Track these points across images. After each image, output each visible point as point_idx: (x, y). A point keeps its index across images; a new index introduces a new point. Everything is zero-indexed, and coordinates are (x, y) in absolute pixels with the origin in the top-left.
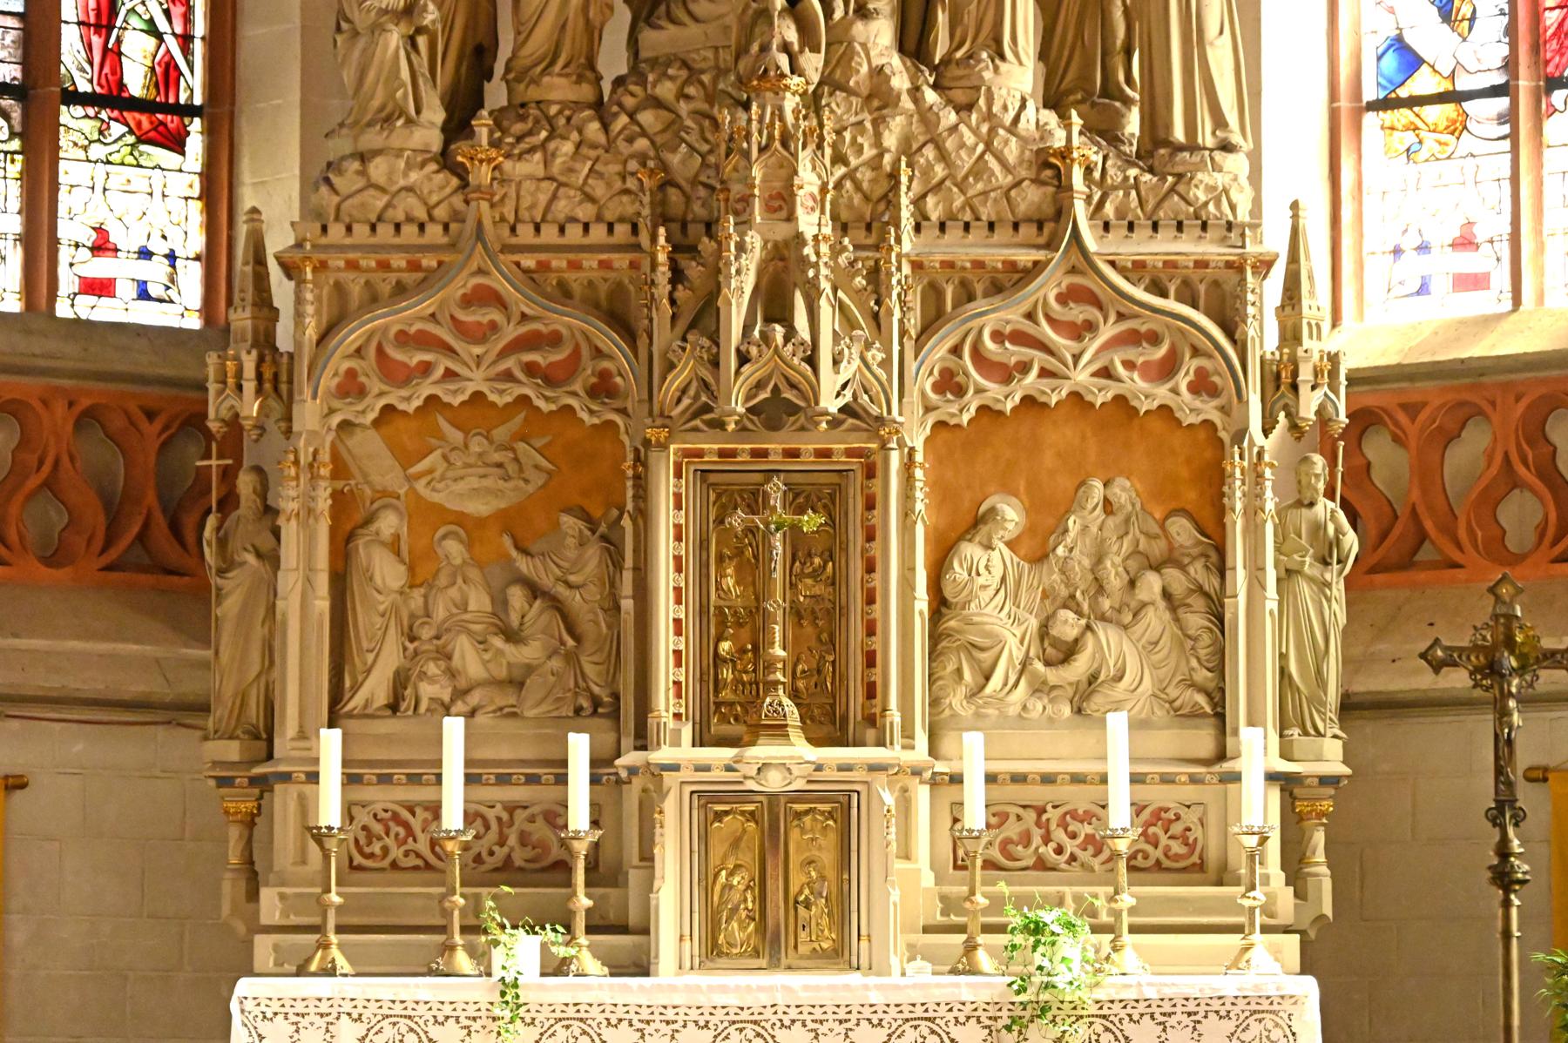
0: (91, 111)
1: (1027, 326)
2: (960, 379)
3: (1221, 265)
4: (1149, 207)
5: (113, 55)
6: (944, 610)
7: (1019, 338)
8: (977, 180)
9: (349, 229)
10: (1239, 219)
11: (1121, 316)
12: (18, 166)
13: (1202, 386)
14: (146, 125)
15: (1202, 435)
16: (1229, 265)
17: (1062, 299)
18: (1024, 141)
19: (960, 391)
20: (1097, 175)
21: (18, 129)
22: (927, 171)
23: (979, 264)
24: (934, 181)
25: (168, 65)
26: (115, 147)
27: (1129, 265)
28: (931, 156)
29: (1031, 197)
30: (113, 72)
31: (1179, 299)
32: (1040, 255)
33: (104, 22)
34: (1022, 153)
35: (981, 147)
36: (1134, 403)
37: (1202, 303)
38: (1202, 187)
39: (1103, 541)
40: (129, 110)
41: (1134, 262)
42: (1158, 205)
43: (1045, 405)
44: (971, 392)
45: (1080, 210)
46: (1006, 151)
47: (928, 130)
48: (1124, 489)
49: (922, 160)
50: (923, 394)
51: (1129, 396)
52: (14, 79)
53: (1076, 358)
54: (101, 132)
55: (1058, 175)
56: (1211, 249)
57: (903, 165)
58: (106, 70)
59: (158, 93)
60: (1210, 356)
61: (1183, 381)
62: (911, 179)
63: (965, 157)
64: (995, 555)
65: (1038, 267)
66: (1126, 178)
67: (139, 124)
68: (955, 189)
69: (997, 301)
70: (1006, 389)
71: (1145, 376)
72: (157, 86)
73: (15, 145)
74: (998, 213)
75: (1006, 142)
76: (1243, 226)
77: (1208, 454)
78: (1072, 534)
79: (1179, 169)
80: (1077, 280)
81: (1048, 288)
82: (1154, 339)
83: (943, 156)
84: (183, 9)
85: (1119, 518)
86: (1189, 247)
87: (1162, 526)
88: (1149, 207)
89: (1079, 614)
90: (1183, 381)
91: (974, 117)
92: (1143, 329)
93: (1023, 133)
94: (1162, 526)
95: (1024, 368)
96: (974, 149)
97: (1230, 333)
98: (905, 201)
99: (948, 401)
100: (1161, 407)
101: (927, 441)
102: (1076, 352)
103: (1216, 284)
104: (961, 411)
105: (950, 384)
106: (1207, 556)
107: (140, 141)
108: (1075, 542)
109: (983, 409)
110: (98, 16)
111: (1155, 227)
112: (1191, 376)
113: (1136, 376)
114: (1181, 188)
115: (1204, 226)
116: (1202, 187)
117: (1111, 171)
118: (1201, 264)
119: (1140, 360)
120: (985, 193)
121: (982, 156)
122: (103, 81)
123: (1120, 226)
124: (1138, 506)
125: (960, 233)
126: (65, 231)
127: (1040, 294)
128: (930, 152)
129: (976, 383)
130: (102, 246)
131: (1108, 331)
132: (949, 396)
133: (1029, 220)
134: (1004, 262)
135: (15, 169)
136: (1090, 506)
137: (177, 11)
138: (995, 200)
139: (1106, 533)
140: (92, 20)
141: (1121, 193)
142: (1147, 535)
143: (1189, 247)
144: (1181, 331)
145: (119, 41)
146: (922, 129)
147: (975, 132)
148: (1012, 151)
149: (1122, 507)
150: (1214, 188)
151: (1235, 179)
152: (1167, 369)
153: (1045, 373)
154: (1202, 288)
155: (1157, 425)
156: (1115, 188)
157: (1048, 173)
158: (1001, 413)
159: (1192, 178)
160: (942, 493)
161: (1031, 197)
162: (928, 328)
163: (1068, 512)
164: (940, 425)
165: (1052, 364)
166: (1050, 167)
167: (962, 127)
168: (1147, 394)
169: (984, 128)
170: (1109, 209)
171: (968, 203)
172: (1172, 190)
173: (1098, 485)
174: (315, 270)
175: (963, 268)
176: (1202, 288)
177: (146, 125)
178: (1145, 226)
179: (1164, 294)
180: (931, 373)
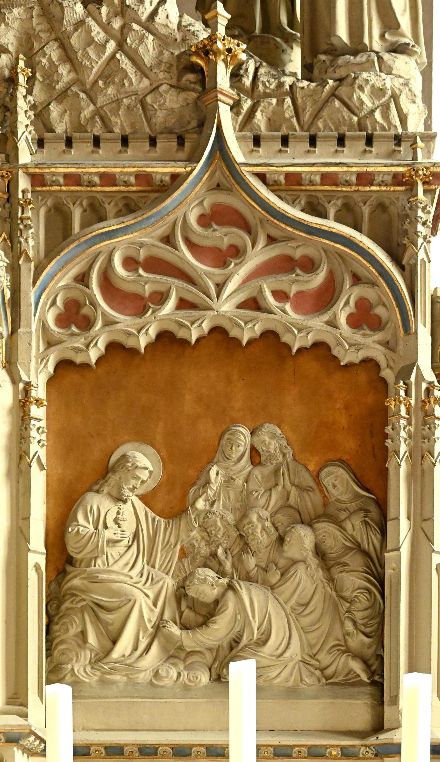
1: (164, 252)
2: (86, 310)
3: (388, 179)
4: (307, 117)
6: (69, 568)
7: (155, 265)
8: (107, 84)
10: (411, 128)
11: (271, 240)
13: (364, 318)
15: (363, 377)
16: (397, 180)
17: (205, 221)
18: (164, 41)
19: (86, 324)
20: (247, 81)
22: (51, 76)
23: (108, 179)
24: (59, 86)
27: (282, 179)
28: (55, 58)
29: (170, 103)
31: (338, 219)
32: (179, 169)
34: (161, 53)
35: (111, 46)
36: (286, 338)
37: (365, 226)
38: (367, 89)
39: (249, 493)
41: (288, 175)
42: (316, 116)
43: (185, 342)
44: (99, 325)
45: (225, 113)
46: (141, 49)
47: (52, 29)
48: (273, 436)
49: (44, 61)
50: (44, 326)
51: (279, 330)
53: (220, 287)
55: (202, 82)
56: (376, 162)
57: (22, 64)
60: (373, 284)
61: (342, 313)
62: (31, 80)
63: (93, 56)
64: (127, 509)
65: (176, 179)
66: (281, 85)
68: (82, 95)
69: (129, 220)
70: (139, 321)
71: (297, 308)
74: (132, 125)
75: (142, 39)
76: (413, 139)
77: (370, 399)
78: (214, 486)
79: (341, 73)
80: (223, 198)
81: (188, 204)
82: (309, 266)
83: (68, 55)
85: (270, 468)
86: (352, 160)
87: (317, 478)
88: (307, 117)
89: (222, 573)
90: (342, 313)
91: (104, 10)
92: (298, 254)
93: (162, 31)
94: (317, 478)
95: (160, 298)
96: (104, 46)
97: (397, 260)
98: (22, 105)
99: (73, 335)
100: (317, 345)
101: (50, 382)
102: (219, 280)
103: (381, 207)
104: (88, 346)
105: (75, 316)
106: (367, 511)
108: (218, 494)
109: (113, 347)
111: (313, 141)
112: (351, 308)
113: (288, 307)
114: (343, 91)
115: (369, 141)
116: (367, 89)
117: (263, 78)
118: (365, 179)
119: (294, 290)
120: (118, 102)
121: (113, 57)
123: (272, 139)
124: (290, 456)
125: (90, 147)
127: (179, 213)
128: (53, 52)
129: (104, 314)
131: (258, 255)
132: (74, 329)
133: (169, 131)
134: (138, 176)
136: (235, 456)
138: (129, 108)
139: (252, 486)
141: (274, 101)
142: (301, 488)
143: (352, 160)
144: (341, 256)
146: (45, 26)
147: (106, 28)
148: (148, 50)
149: (271, 457)
150: (381, 91)
151: (406, 84)
152: (324, 299)
153: (183, 304)
154: (366, 210)
155: (310, 366)
156: (268, 96)
157: (191, 77)
158: (134, 351)
159: (355, 78)
160: (65, 442)
161: (170, 103)
162: (51, 251)
163: (210, 462)
164: (63, 365)
165: (193, 294)
166: (192, 69)
167: (90, 21)
168: (302, 329)
169: (117, 24)
170: (260, 118)
171: (98, 113)
172: (333, 94)
173: (243, 434)
175: (91, 184)
176: (366, 210)
178: (300, 139)
179: (324, 215)
180: (54, 303)
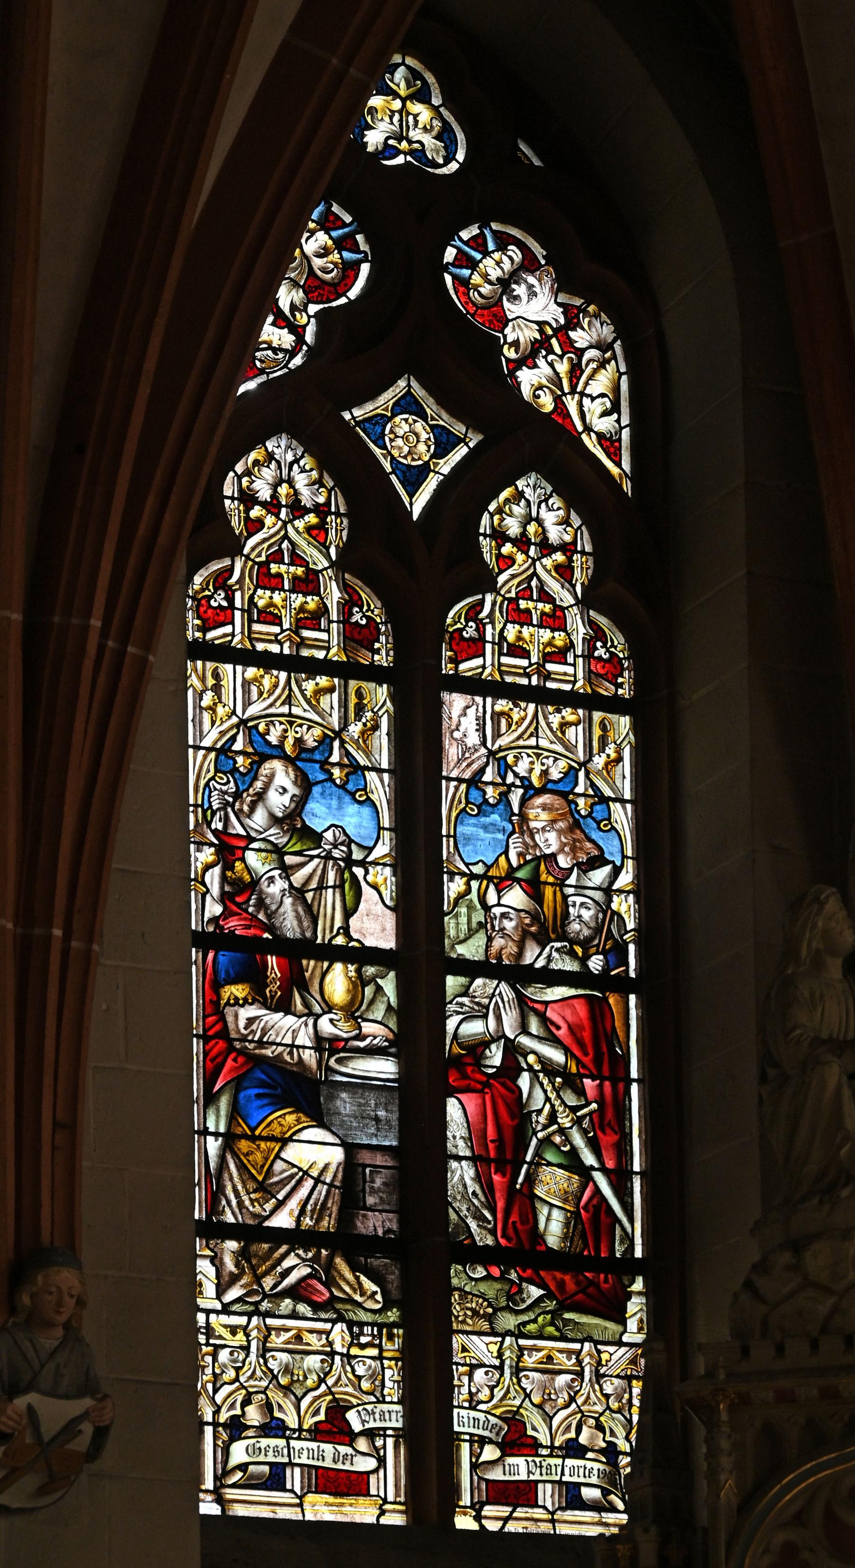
0: (496, 1272)
5: (524, 1201)
9: (780, 1349)
12: (398, 1343)
14: (571, 1286)
21: (395, 1295)
25: (597, 1208)
26: (525, 1318)
30: (524, 1220)
33: (509, 1156)
40: (547, 1268)
52: (389, 1231)
54: (510, 1297)
58: (514, 1218)
59: (586, 1246)
67: (561, 1285)
72: (583, 1236)
73: (393, 1315)
84: (616, 1138)
107: (564, 1306)
110: (500, 1149)
122: (510, 1231)
126: (463, 1420)
130: (516, 1439)
135: (391, 1348)
137: (608, 1140)
140: (492, 1154)
145: (531, 1180)
174: (731, 1408)
177: (571, 1286)
